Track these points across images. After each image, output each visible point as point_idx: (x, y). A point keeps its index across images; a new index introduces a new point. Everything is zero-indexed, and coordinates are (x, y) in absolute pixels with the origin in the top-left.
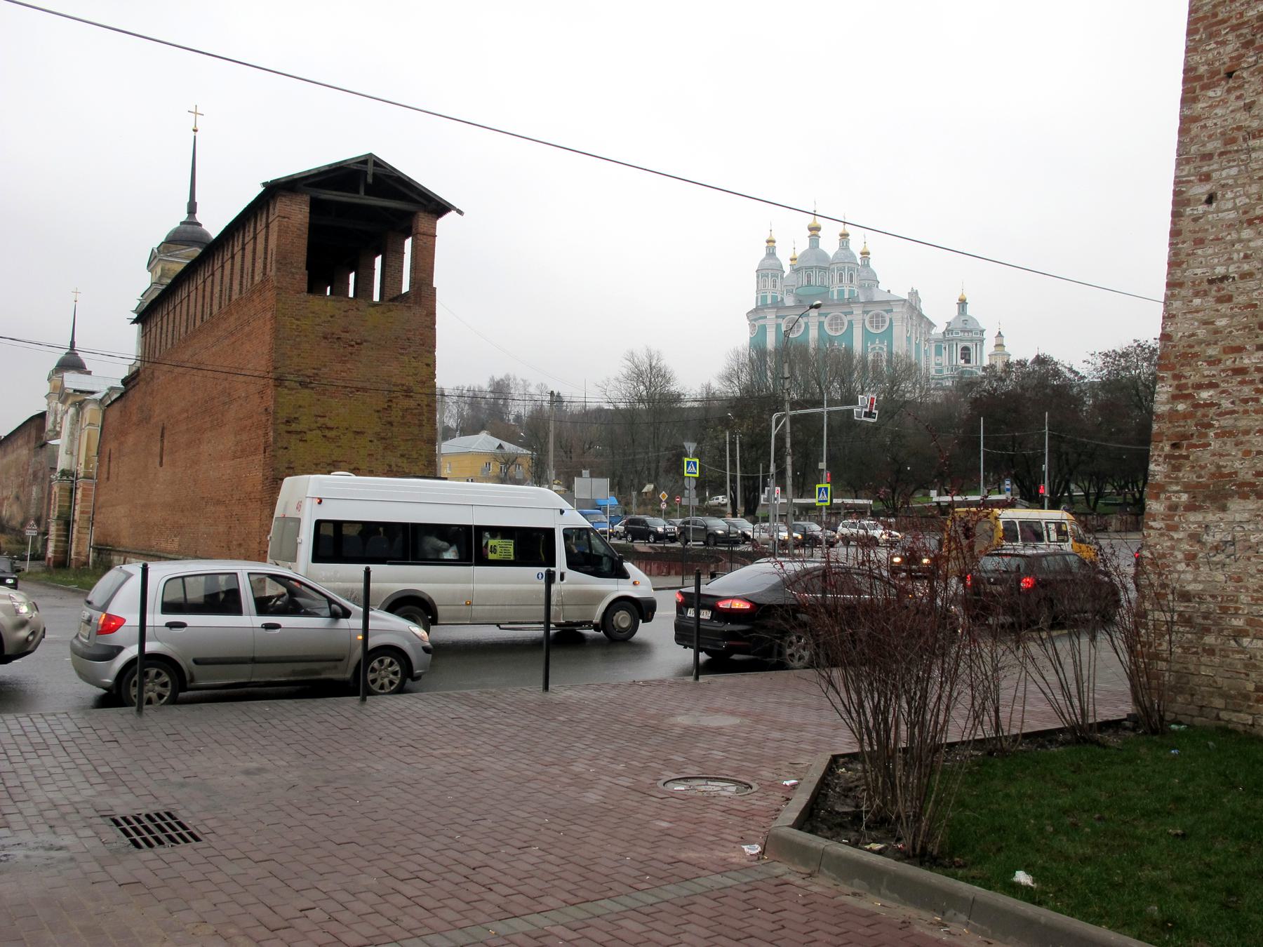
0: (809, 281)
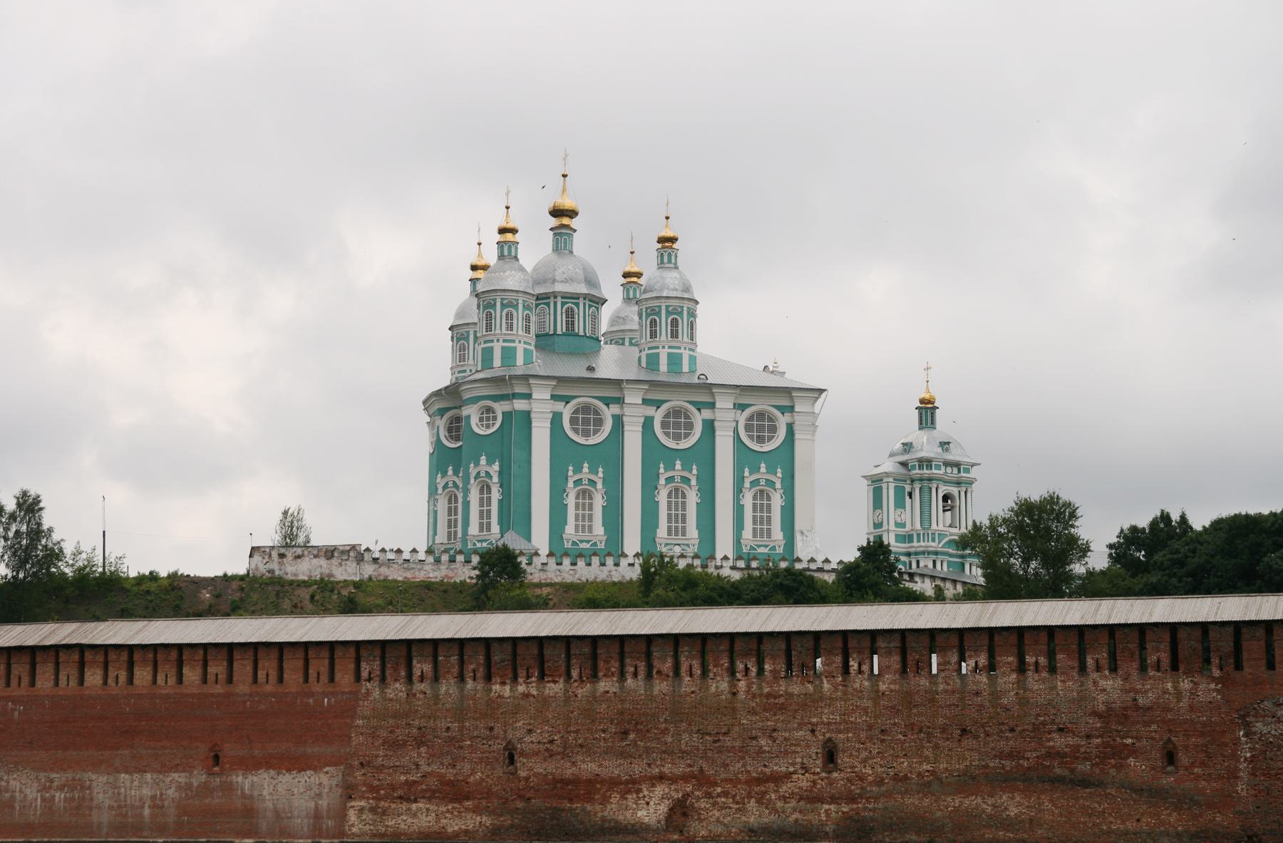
0: (570, 324)
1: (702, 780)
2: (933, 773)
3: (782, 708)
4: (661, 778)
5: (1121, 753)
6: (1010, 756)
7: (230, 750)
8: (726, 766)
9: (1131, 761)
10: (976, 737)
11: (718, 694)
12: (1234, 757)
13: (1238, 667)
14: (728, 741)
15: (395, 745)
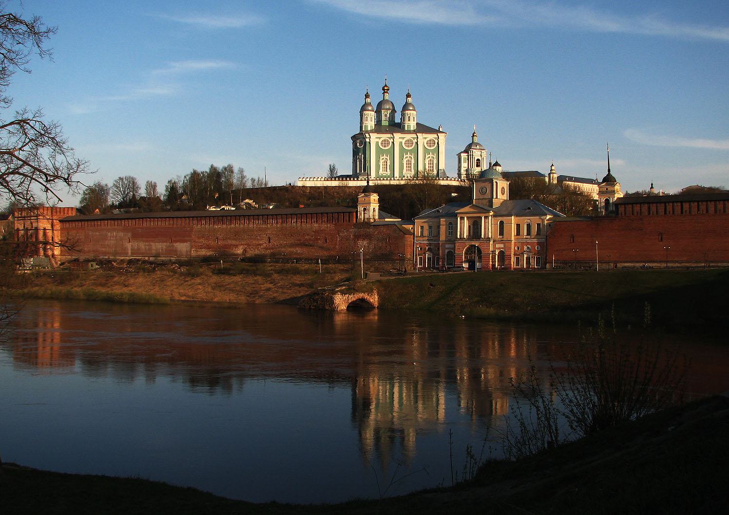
4: (242, 244)
5: (318, 239)
6: (299, 240)
7: (173, 239)
15: (199, 238)
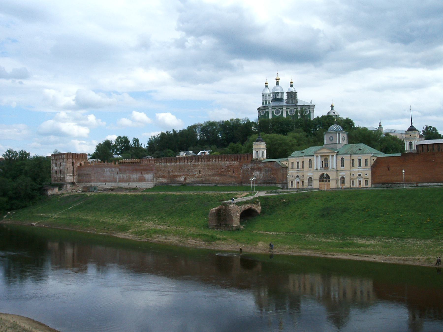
1: (187, 175)
2: (210, 174)
3: (195, 166)
4: (183, 175)
8: (189, 173)
9: (230, 172)
10: (214, 170)
11: (189, 164)
12: (240, 172)
13: (241, 160)
14: (190, 170)
